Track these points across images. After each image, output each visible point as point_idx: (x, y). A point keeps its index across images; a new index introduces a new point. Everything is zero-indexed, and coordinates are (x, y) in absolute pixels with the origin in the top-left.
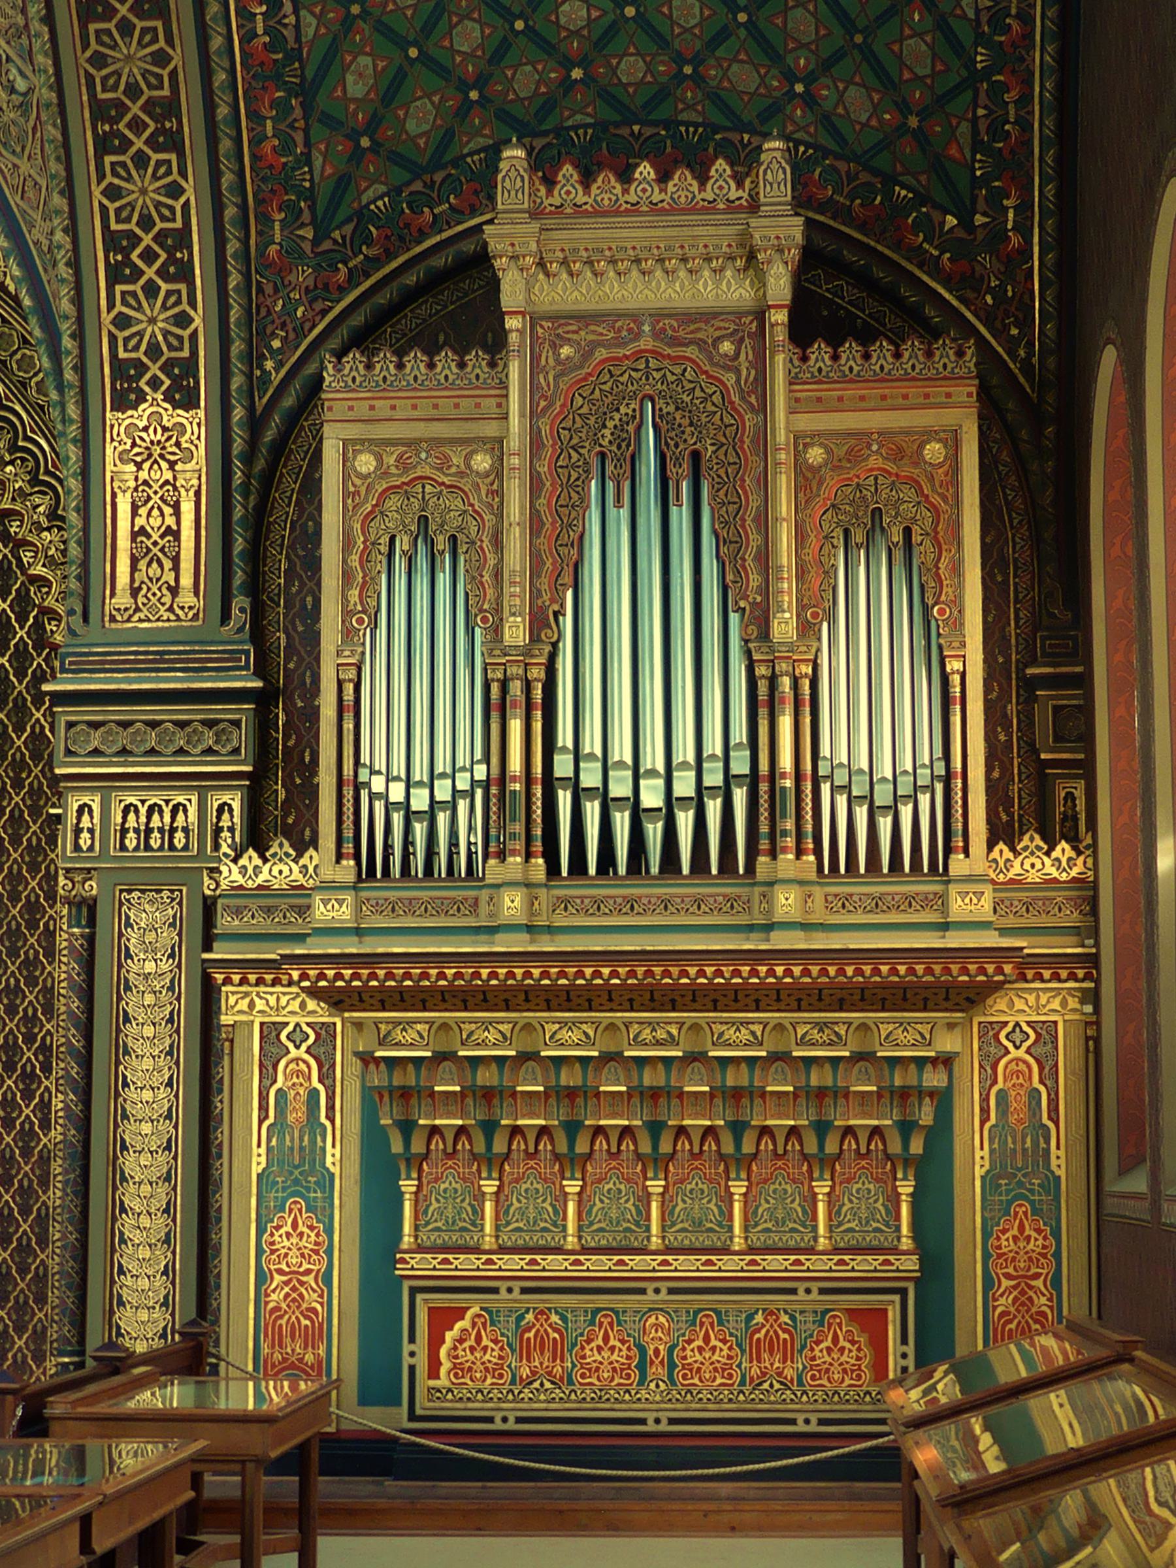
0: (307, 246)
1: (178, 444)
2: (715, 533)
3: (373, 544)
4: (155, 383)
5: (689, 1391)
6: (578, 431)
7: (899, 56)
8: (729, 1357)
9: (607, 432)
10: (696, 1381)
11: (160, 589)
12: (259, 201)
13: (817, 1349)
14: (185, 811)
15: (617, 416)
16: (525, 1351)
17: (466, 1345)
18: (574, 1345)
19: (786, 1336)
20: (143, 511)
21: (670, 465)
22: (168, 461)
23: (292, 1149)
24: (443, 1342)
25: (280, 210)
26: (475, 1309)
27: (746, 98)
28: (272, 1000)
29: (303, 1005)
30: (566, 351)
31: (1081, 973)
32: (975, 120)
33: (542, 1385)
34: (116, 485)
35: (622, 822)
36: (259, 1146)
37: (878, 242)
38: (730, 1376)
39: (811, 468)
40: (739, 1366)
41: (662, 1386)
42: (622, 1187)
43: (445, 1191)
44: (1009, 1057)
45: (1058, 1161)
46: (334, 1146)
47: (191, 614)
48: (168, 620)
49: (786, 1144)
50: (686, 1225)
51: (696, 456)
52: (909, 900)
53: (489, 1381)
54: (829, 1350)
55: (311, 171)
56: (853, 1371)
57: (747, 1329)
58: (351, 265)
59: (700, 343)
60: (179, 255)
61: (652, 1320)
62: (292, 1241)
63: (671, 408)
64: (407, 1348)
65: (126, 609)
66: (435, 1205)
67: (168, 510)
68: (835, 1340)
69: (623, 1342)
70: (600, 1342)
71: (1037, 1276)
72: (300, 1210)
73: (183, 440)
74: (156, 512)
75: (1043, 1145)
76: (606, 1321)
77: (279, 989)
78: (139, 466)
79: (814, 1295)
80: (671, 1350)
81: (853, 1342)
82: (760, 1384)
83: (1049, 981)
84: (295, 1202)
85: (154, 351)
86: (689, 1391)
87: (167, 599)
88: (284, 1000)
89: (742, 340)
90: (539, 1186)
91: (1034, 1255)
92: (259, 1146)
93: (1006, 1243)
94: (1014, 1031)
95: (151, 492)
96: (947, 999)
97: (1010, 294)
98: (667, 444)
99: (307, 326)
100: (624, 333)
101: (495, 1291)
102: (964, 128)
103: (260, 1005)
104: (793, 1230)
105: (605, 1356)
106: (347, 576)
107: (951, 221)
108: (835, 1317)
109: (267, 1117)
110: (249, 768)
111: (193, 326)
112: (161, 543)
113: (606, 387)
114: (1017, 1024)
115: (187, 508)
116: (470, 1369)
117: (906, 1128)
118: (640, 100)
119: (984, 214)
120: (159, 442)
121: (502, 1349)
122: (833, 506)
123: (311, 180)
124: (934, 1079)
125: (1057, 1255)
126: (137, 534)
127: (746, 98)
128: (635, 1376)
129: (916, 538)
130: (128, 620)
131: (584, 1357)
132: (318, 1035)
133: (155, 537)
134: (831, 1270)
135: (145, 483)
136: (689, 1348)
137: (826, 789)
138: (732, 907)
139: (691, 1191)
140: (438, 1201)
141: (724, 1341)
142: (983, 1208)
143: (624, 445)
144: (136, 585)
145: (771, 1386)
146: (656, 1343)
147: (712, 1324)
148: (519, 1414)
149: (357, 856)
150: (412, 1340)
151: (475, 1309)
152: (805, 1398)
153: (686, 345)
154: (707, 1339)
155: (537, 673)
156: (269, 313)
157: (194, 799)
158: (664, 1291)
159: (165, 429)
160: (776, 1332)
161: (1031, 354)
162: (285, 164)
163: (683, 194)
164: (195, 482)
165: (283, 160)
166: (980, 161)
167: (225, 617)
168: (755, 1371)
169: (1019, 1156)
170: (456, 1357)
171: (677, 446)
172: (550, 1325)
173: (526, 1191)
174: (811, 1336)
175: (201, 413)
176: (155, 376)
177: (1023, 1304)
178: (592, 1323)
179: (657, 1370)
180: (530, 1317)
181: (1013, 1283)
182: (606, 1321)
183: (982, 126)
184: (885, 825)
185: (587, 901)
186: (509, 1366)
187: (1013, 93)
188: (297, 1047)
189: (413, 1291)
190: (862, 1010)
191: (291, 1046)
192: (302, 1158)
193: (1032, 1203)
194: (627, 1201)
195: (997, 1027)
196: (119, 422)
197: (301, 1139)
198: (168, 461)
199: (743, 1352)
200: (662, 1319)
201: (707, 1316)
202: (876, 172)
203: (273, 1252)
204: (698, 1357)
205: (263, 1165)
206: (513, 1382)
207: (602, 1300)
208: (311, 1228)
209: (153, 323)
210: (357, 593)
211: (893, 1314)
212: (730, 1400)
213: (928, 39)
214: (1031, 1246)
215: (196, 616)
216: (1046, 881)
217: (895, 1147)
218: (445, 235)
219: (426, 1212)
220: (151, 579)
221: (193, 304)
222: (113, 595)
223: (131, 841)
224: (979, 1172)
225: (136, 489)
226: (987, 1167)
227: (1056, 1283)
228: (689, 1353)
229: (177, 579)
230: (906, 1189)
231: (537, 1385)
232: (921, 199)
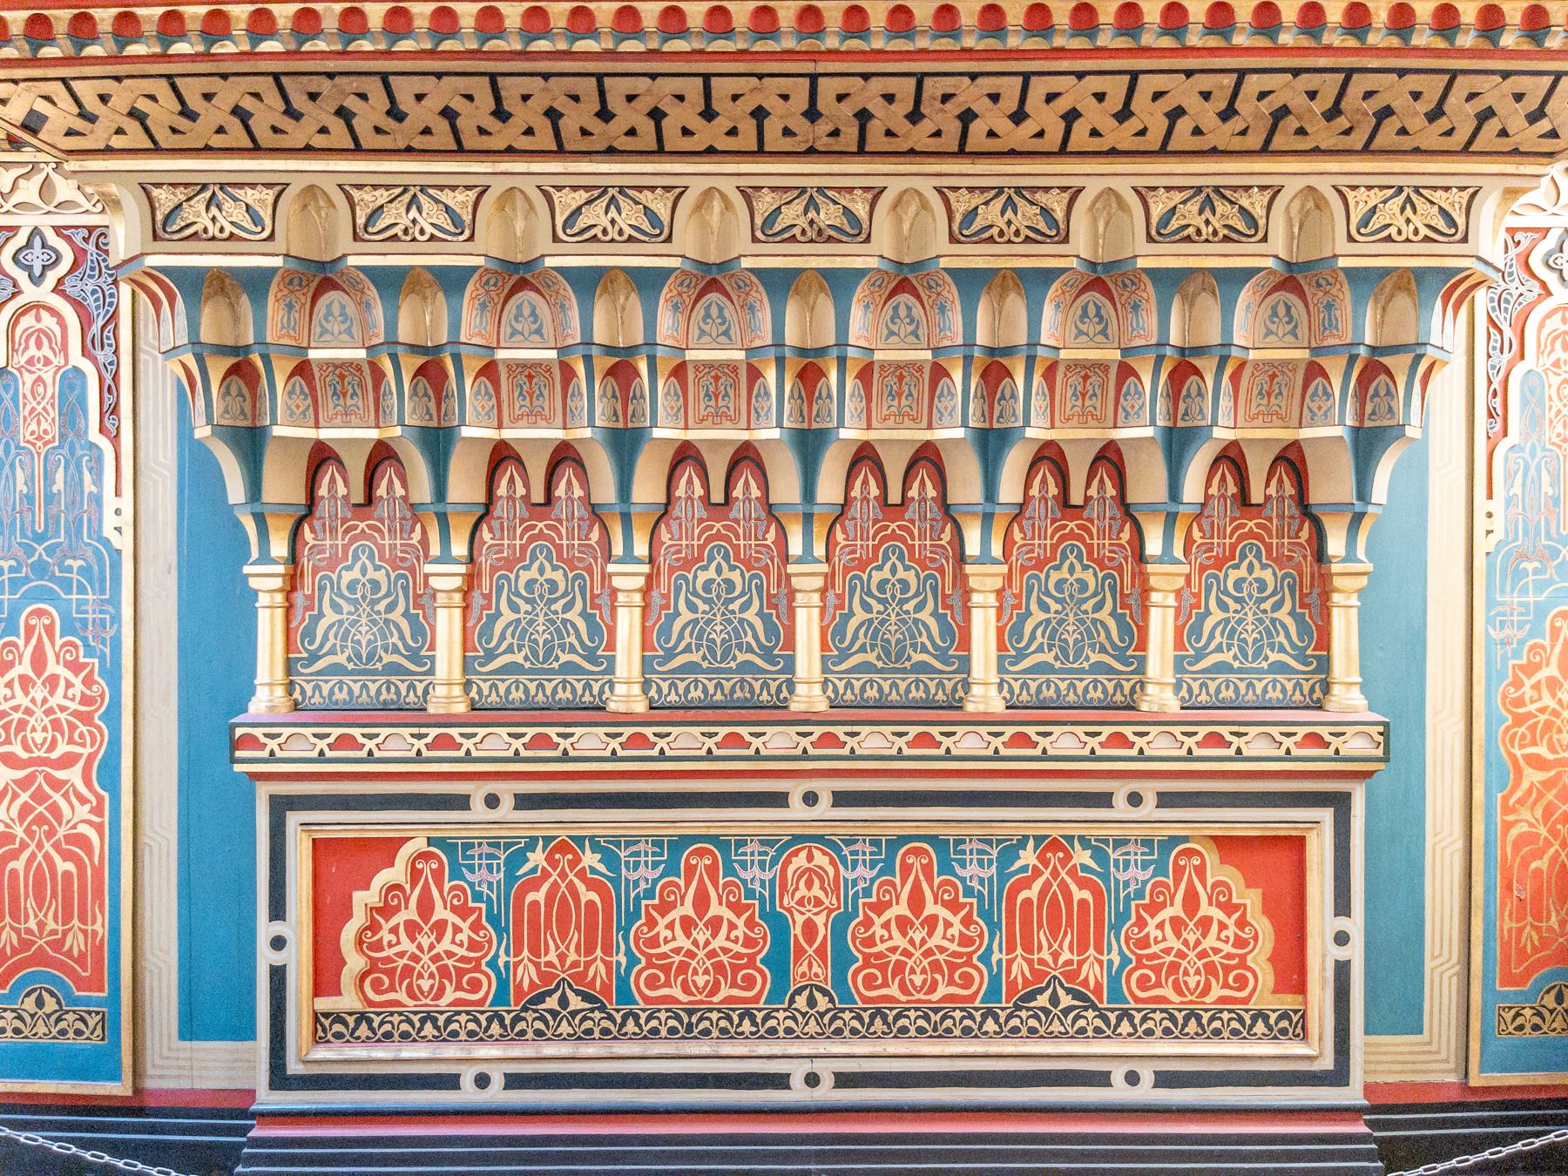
8: (965, 941)
10: (894, 990)
13: (1152, 923)
16: (528, 931)
17: (399, 918)
18: (633, 916)
19: (1086, 895)
23: (29, 498)
24: (348, 915)
33: (564, 1002)
38: (967, 981)
40: (986, 958)
41: (822, 1003)
42: (735, 576)
43: (352, 586)
49: (1088, 486)
50: (871, 657)
53: (450, 995)
54: (1177, 924)
56: (1227, 969)
61: (800, 861)
66: (330, 617)
69: (737, 908)
70: (688, 909)
72: (49, 630)
79: (1149, 809)
80: (840, 926)
81: (1229, 908)
82: (1031, 996)
84: (39, 613)
90: (558, 576)
101: (462, 802)
108: (1190, 853)
116: (407, 971)
128: (764, 983)
131: (654, 942)
139: (882, 585)
141: (954, 906)
145: (1054, 1000)
146: (808, 910)
147: (927, 870)
150: (278, 910)
151: (418, 844)
154: (916, 902)
158: (825, 800)
160: (1063, 886)
168: (1020, 968)
170: (378, 946)
172: (581, 875)
173: (530, 584)
178: (672, 869)
179: (810, 969)
180: (537, 858)
186: (493, 964)
188: (36, 281)
189: (281, 806)
192: (52, 520)
194: (745, 607)
197: (49, 479)
199: (994, 927)
200: (821, 859)
201: (917, 852)
204: (899, 941)
206: (501, 997)
208: (75, 667)
219: (309, 633)
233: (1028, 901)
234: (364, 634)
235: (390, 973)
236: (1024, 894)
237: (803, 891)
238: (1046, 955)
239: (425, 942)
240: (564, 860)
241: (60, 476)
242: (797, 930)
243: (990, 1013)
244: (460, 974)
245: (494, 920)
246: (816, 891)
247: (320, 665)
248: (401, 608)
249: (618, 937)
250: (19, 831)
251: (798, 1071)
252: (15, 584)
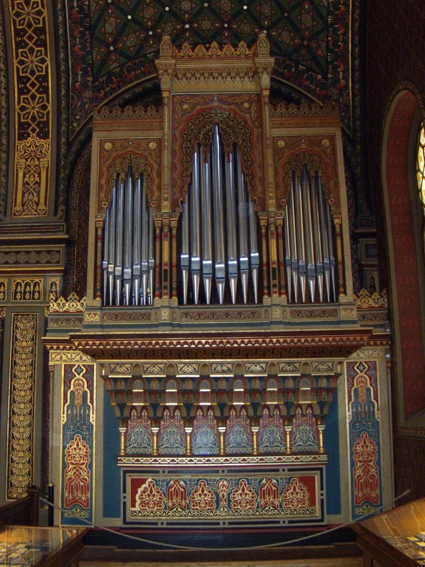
0: (90, 84)
1: (41, 152)
2: (243, 172)
3: (111, 176)
4: (33, 130)
5: (237, 511)
6: (190, 135)
7: (301, 21)
8: (252, 497)
9: (201, 135)
10: (239, 507)
11: (32, 204)
12: (73, 67)
13: (287, 493)
14: (39, 285)
15: (205, 130)
16: (170, 496)
17: (147, 493)
18: (190, 494)
19: (275, 488)
20: (27, 176)
21: (225, 147)
22: (37, 158)
23: (76, 415)
24: (137, 492)
25: (81, 70)
26: (150, 479)
27: (246, 35)
28: (69, 356)
29: (81, 358)
30: (185, 106)
31: (384, 342)
32: (328, 41)
33: (177, 509)
34: (18, 166)
36: (64, 413)
37: (293, 84)
38: (253, 505)
39: (280, 149)
40: (256, 501)
41: (226, 509)
43: (137, 432)
44: (358, 376)
45: (378, 415)
46: (93, 414)
47: (43, 212)
48: (35, 215)
51: (235, 145)
52: (324, 313)
53: (156, 508)
55: (92, 57)
57: (259, 485)
58: (105, 90)
59: (236, 104)
60: (44, 84)
61: (221, 483)
62: (77, 449)
63: (225, 127)
64: (122, 495)
65: (20, 211)
66: (133, 437)
67: (36, 175)
68: (295, 489)
69: (209, 492)
71: (371, 461)
72: (80, 439)
73: (43, 150)
74: (32, 176)
75: (372, 409)
76: (202, 484)
77: (71, 351)
78: (27, 160)
80: (229, 495)
81: (301, 490)
83: (373, 346)
85: (33, 119)
86: (237, 511)
87: (35, 207)
88: (74, 356)
89: (252, 103)
91: (370, 453)
92: (64, 413)
93: (359, 448)
94: (360, 365)
95: (30, 169)
96: (340, 352)
97: (341, 101)
98: (224, 139)
99: (89, 112)
100: (207, 100)
102: (324, 44)
103: (64, 357)
104: (277, 446)
105: (203, 497)
106: (100, 187)
107: (320, 77)
108: (294, 480)
109: (67, 402)
110: (63, 268)
111: (48, 109)
112: (34, 187)
113: (201, 119)
114: (361, 363)
115: (43, 175)
118: (209, 36)
119: (331, 74)
120: (34, 151)
121: (161, 495)
122: (288, 162)
123: (92, 60)
126: (25, 184)
127: (246, 35)
128: (215, 506)
129: (320, 174)
130: (20, 215)
131: (194, 498)
132: (87, 370)
133: (31, 185)
134: (293, 462)
135: (29, 166)
136: (236, 494)
137: (288, 269)
138: (254, 316)
140: (134, 436)
142: (350, 435)
143: (207, 140)
144: (24, 202)
145: (269, 508)
146: (223, 492)
148: (168, 521)
149: (102, 297)
150: (124, 491)
151: (150, 479)
152: (283, 513)
153: (231, 105)
154: (243, 490)
155: (174, 224)
156: (75, 107)
157: (42, 280)
159: (36, 146)
160: (271, 487)
161: (349, 122)
162: (83, 54)
163: (229, 52)
164: (47, 165)
165: (82, 53)
166: (330, 56)
167: (56, 213)
168: (263, 503)
169: (363, 415)
170: (142, 499)
171: (228, 140)
172: (180, 486)
173: (170, 432)
174: (285, 488)
175: (49, 140)
176: (34, 128)
177: (366, 472)
178: (197, 484)
179: (224, 503)
180: (172, 482)
181: (361, 464)
182: (202, 484)
183: (330, 43)
185: (195, 314)
186: (164, 502)
187: (341, 31)
188: (79, 374)
189: (125, 472)
190: (306, 357)
191: (76, 374)
192: (81, 419)
193: (368, 432)
195: (353, 364)
196: (20, 145)
197: (80, 411)
198: (37, 158)
199: (258, 495)
200: (225, 483)
202: (292, 60)
203: (69, 456)
204: (240, 497)
205: (65, 421)
206: (165, 509)
209: (34, 109)
210: (104, 194)
211: (317, 478)
212: (253, 514)
213: (311, 14)
214: (369, 449)
215: (45, 213)
216: (370, 307)
218: (139, 81)
219: (129, 440)
220: (29, 200)
221: (48, 101)
222: (15, 206)
223: (18, 296)
224: (348, 421)
225: (25, 168)
226: (351, 419)
228: (236, 496)
229: (39, 200)
231: (175, 509)
232: (309, 69)
233: (264, 490)
234: (139, 440)
235: (145, 504)
236: (263, 489)
237: (222, 489)
238: (268, 500)
239: (151, 498)
240: (177, 483)
241: (82, 411)
242: (221, 496)
243: (257, 511)
244: (158, 504)
245: (164, 494)
246: (224, 488)
247: (131, 446)
248: (146, 436)
249: (187, 498)
250: (73, 477)
251: (221, 522)
252: (73, 431)
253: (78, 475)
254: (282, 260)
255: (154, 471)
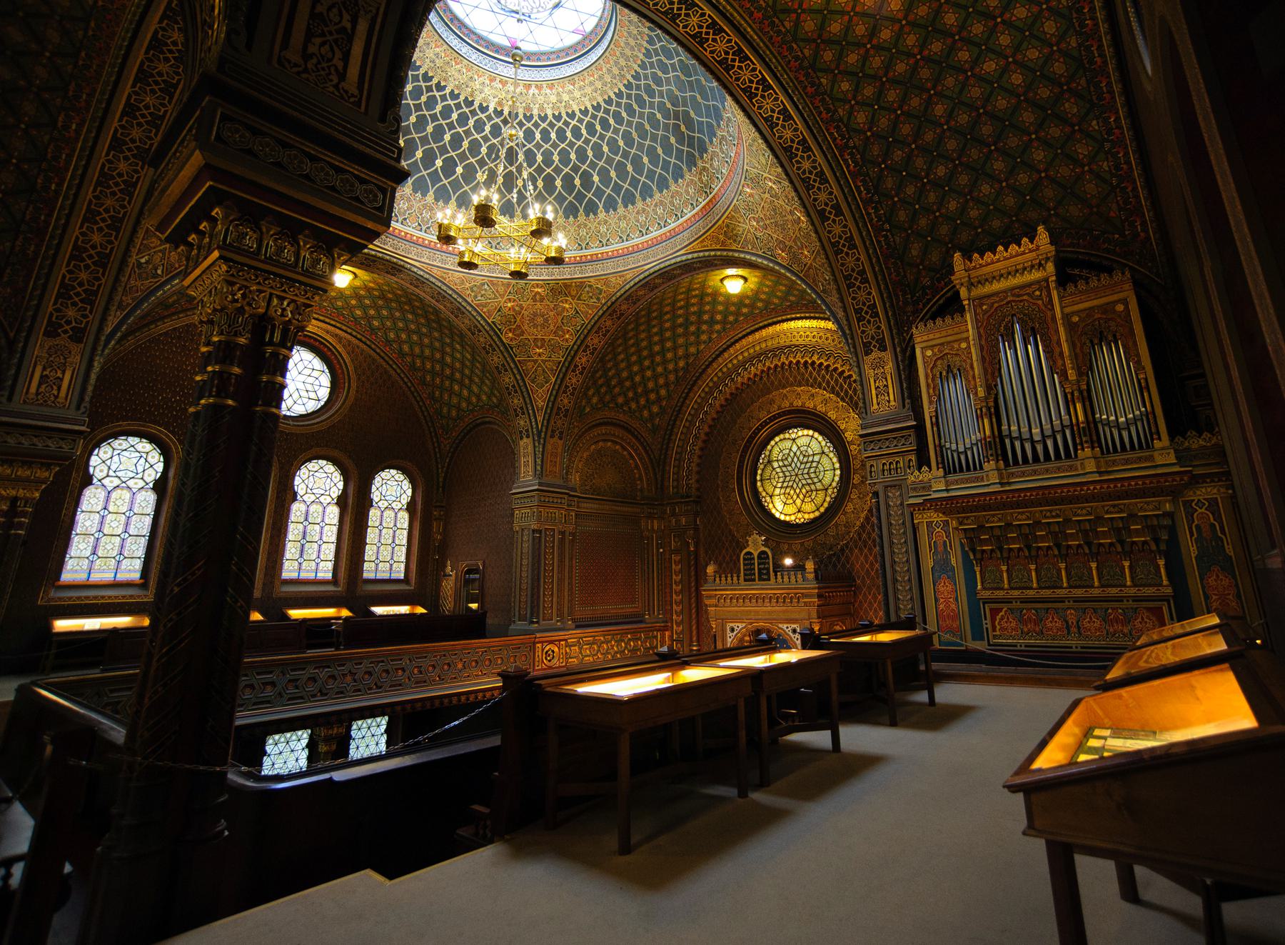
35: (1028, 446)
62: (945, 587)
117: (1157, 540)
124: (1167, 522)
125: (1237, 585)
184: (1125, 434)
207: (1050, 605)
217: (1154, 547)
227: (1239, 596)
230: (1162, 563)
244: (1016, 629)
253: (947, 606)
254: (1090, 418)
255: (1008, 601)
